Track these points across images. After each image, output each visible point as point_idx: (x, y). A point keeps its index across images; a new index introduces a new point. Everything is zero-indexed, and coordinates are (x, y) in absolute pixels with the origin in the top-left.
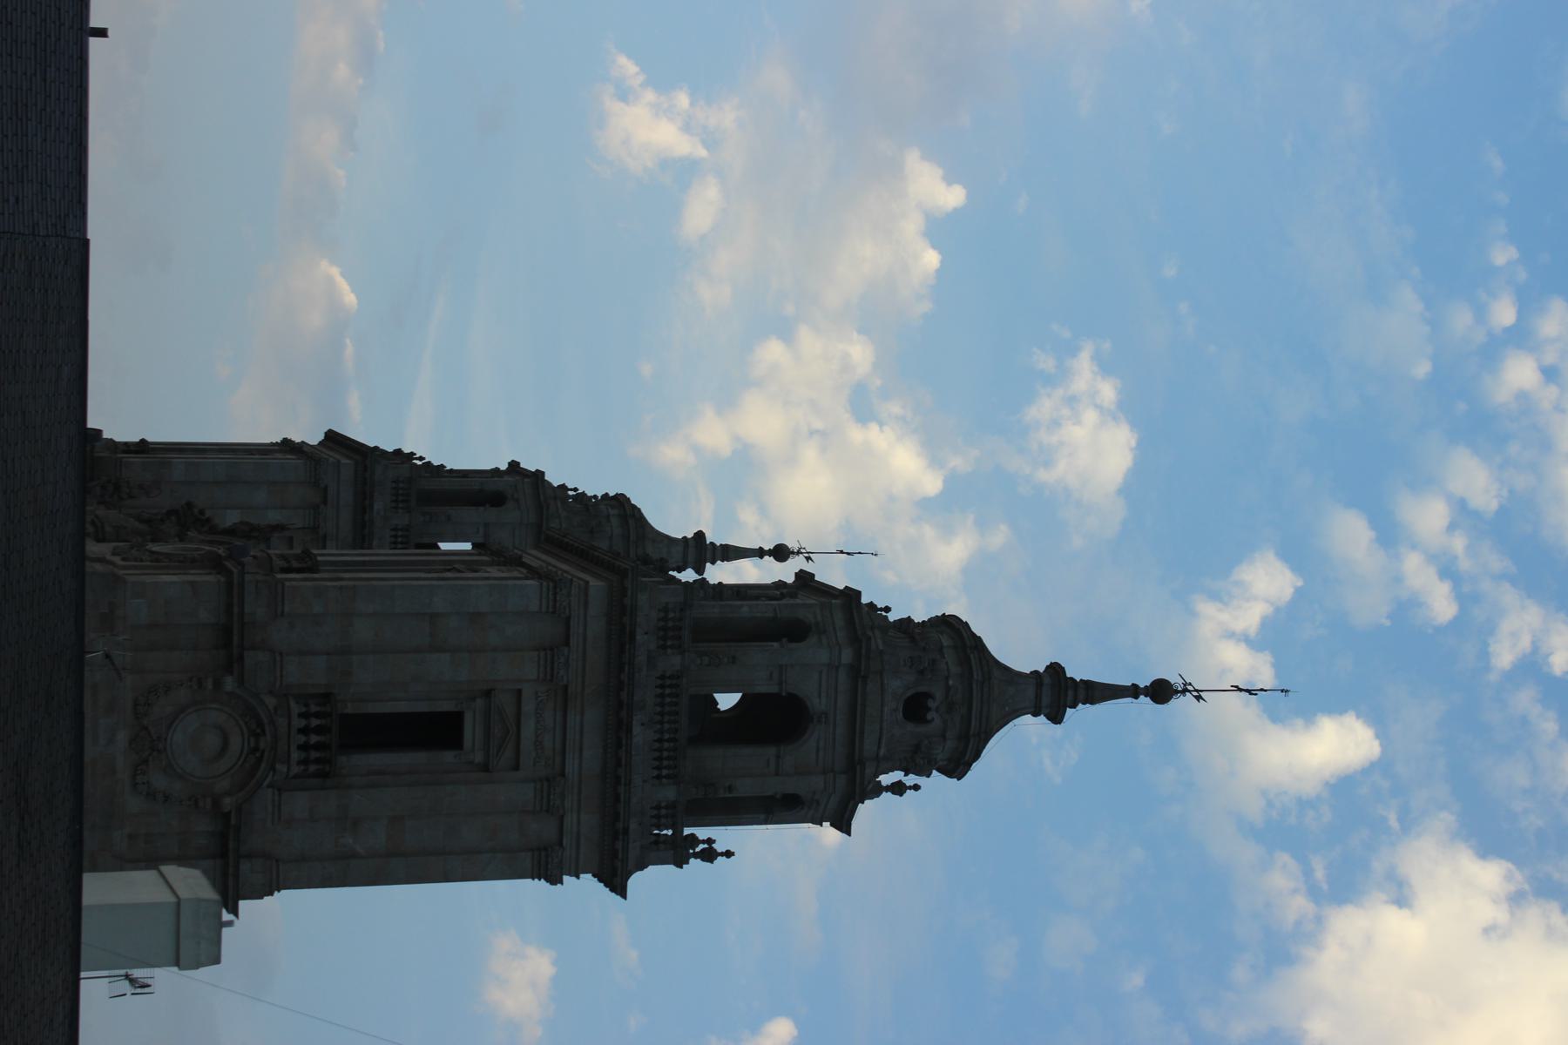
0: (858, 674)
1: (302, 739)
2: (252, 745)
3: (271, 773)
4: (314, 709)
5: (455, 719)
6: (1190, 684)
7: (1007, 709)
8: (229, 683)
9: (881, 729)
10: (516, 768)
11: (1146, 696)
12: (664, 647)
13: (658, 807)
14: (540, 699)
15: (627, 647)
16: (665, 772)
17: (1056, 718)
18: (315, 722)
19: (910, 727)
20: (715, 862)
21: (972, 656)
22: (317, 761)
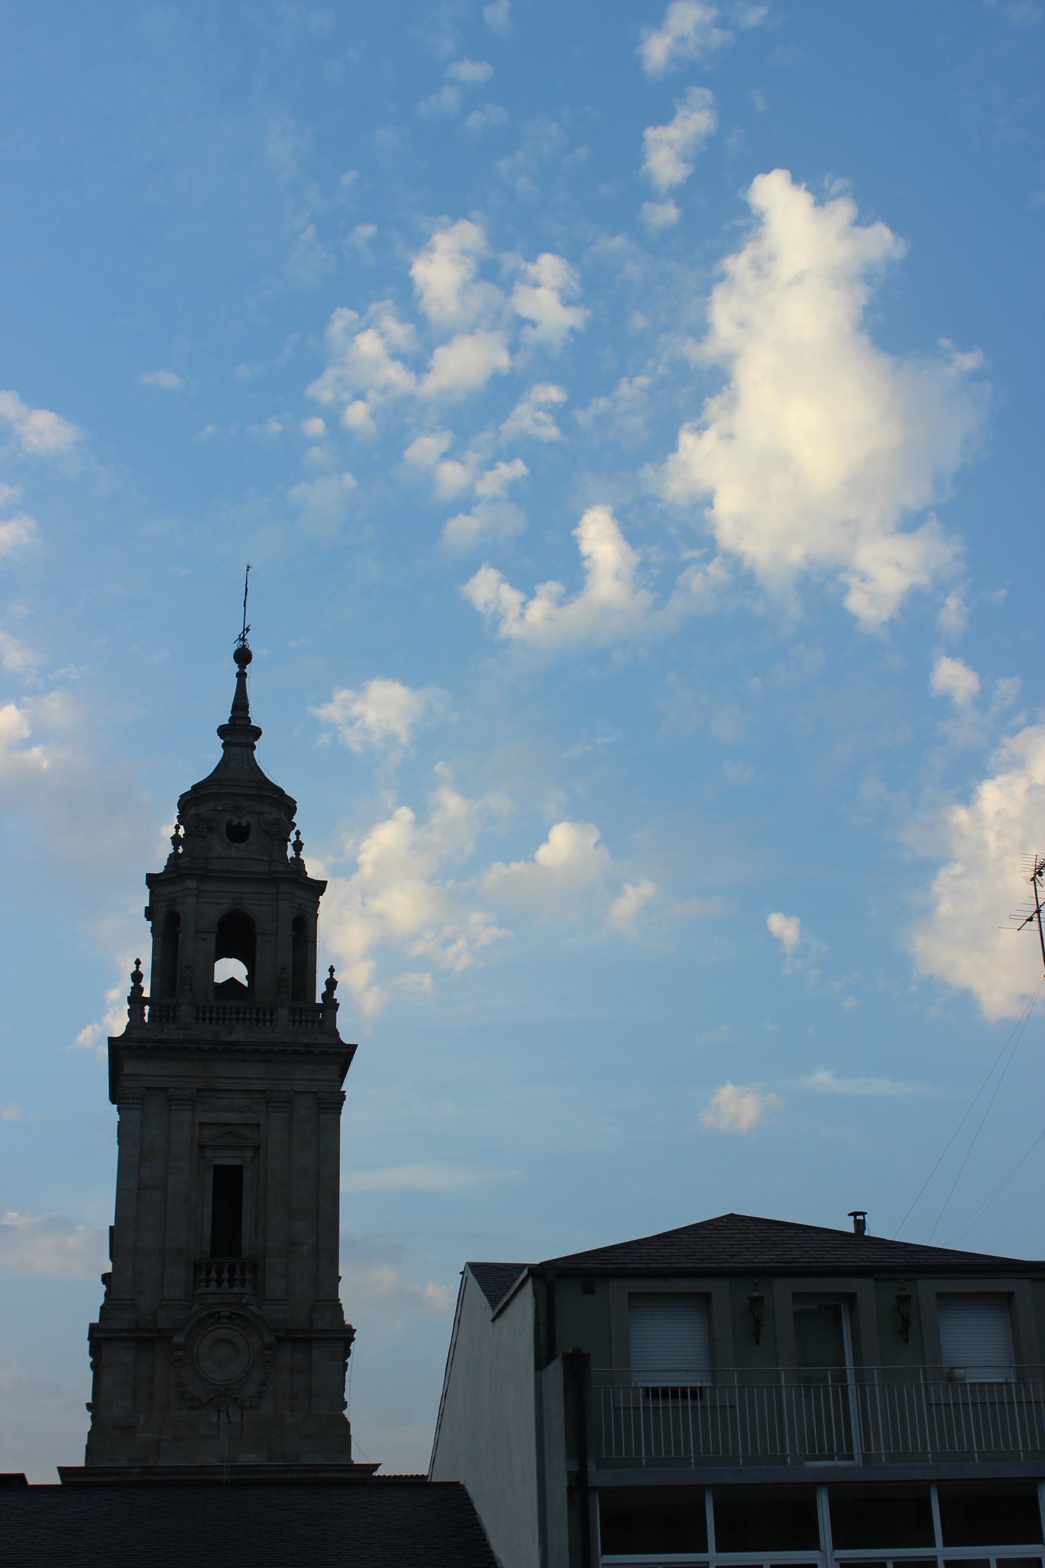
0: (205, 876)
1: (225, 1284)
2: (226, 1321)
3: (249, 1307)
4: (203, 1276)
6: (240, 636)
7: (246, 767)
9: (248, 859)
10: (258, 1125)
11: (246, 667)
13: (294, 1022)
14: (207, 1109)
15: (169, 1045)
16: (268, 1017)
17: (257, 733)
18: (213, 1275)
19: (251, 838)
20: (337, 980)
21: (202, 793)
22: (243, 1272)
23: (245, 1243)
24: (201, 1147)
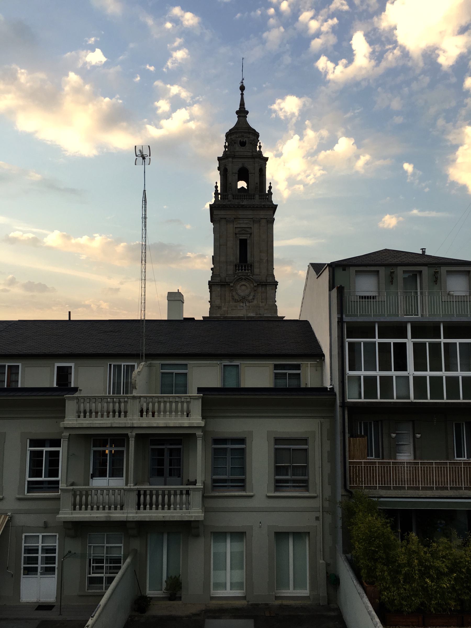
0: (234, 157)
1: (243, 270)
4: (238, 268)
5: (241, 241)
8: (232, 284)
10: (251, 228)
12: (227, 198)
13: (260, 198)
16: (253, 197)
17: (247, 112)
18: (240, 268)
19: (246, 145)
22: (248, 267)
23: (248, 260)
24: (236, 234)
